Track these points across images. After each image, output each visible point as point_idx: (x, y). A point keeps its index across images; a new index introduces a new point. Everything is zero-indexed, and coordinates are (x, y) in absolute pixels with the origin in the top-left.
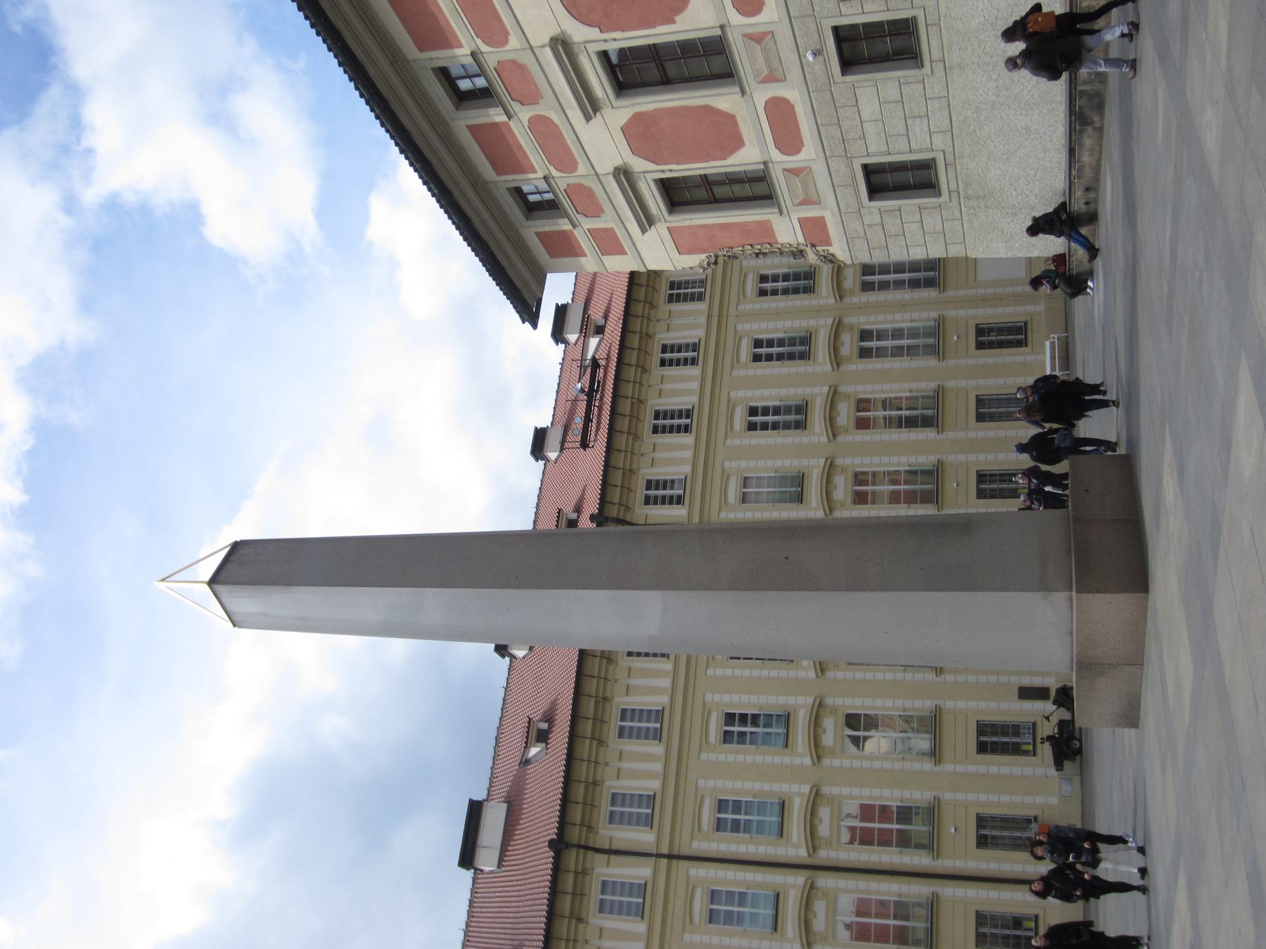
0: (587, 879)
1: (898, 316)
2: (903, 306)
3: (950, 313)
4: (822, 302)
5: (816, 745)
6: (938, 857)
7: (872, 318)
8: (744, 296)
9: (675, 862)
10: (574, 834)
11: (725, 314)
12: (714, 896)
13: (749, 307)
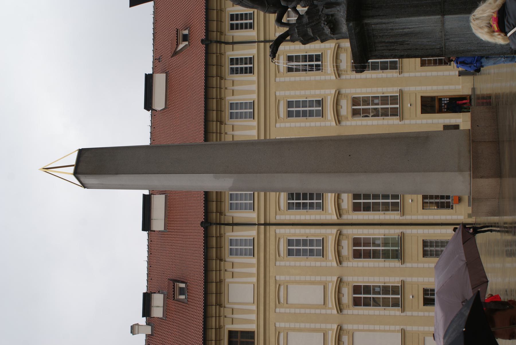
0: (223, 239)
5: (339, 209)
9: (268, 227)
12: (290, 242)
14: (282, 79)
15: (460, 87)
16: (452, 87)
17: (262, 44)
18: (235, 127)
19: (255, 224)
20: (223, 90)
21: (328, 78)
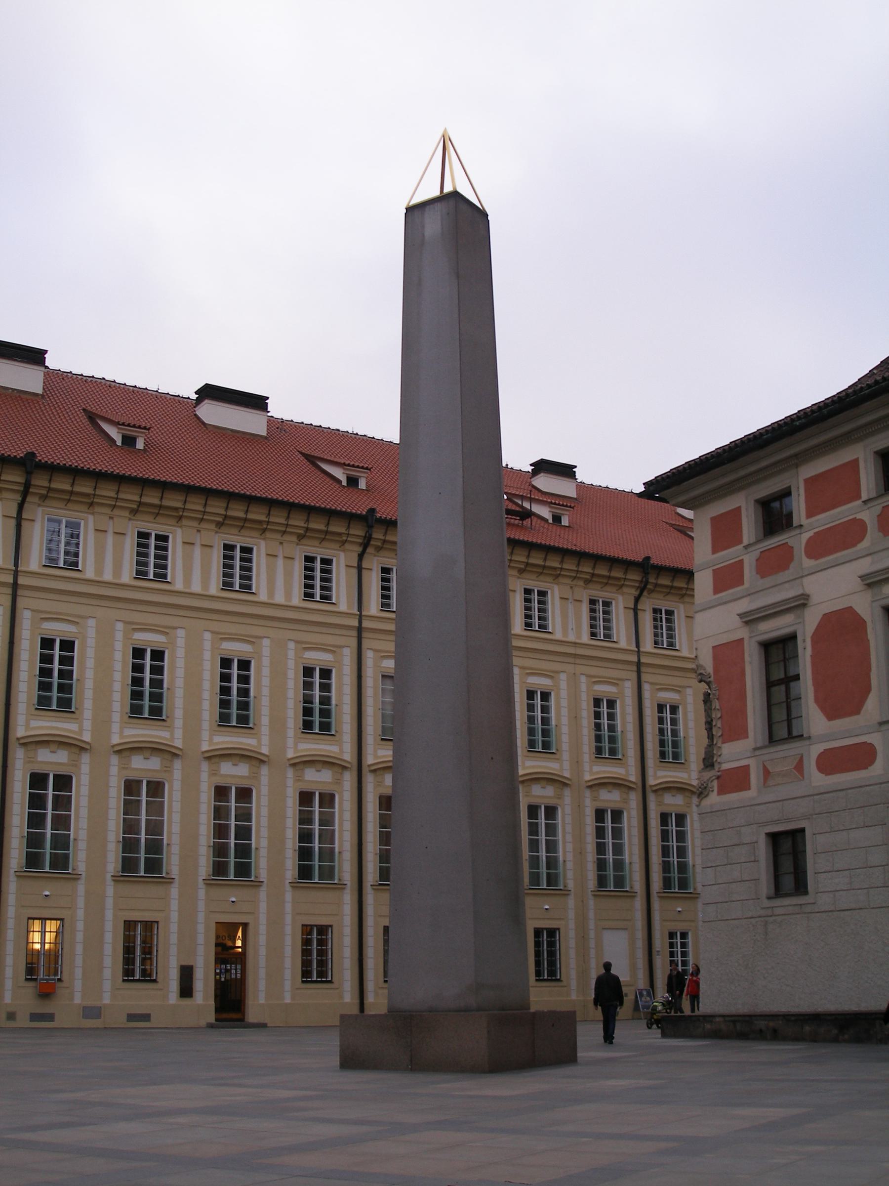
1: (570, 847)
2: (580, 853)
3: (571, 902)
4: (587, 767)
6: (18, 876)
7: (568, 819)
8: (595, 682)
9: (9, 591)
10: (40, 481)
11: (578, 661)
13: (584, 687)
14: (291, 654)
15: (262, 1001)
16: (262, 985)
17: (356, 623)
18: (208, 550)
19: (16, 564)
20: (278, 536)
21: (290, 742)
